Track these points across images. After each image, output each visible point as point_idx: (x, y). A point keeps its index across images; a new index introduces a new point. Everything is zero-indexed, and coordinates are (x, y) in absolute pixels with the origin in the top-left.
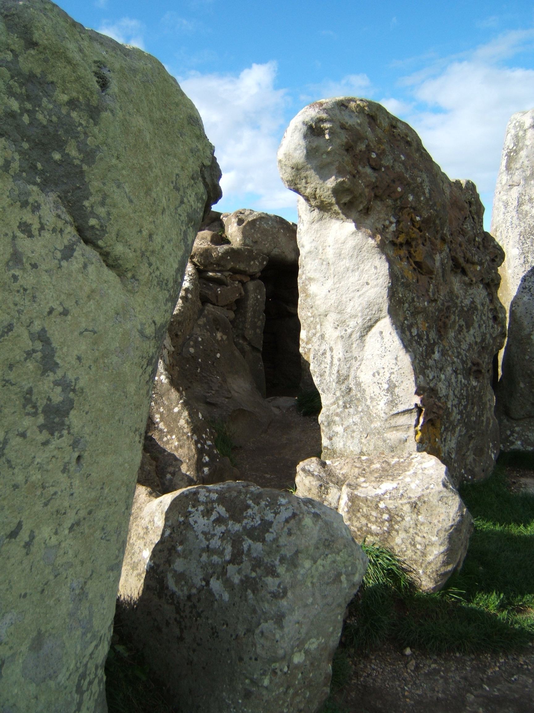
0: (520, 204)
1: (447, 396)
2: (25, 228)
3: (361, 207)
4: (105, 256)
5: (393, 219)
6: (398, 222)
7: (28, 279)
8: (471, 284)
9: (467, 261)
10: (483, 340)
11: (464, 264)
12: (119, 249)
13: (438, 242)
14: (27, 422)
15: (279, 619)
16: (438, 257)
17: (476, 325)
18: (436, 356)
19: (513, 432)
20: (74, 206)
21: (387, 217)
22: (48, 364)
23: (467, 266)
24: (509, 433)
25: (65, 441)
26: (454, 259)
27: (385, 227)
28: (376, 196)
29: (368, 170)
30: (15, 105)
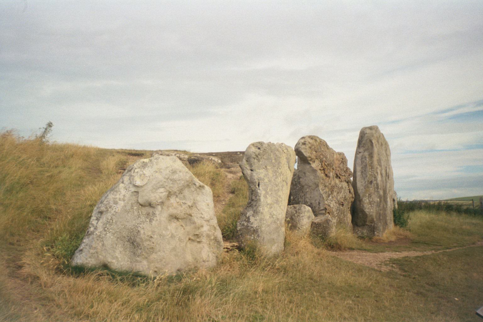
0: (362, 159)
6: (322, 164)
8: (342, 181)
9: (341, 175)
10: (345, 197)
11: (339, 176)
13: (332, 169)
16: (331, 173)
17: (343, 192)
18: (330, 197)
19: (358, 230)
23: (341, 177)
24: (357, 231)
26: (337, 174)
27: (318, 166)
28: (316, 158)
29: (315, 152)
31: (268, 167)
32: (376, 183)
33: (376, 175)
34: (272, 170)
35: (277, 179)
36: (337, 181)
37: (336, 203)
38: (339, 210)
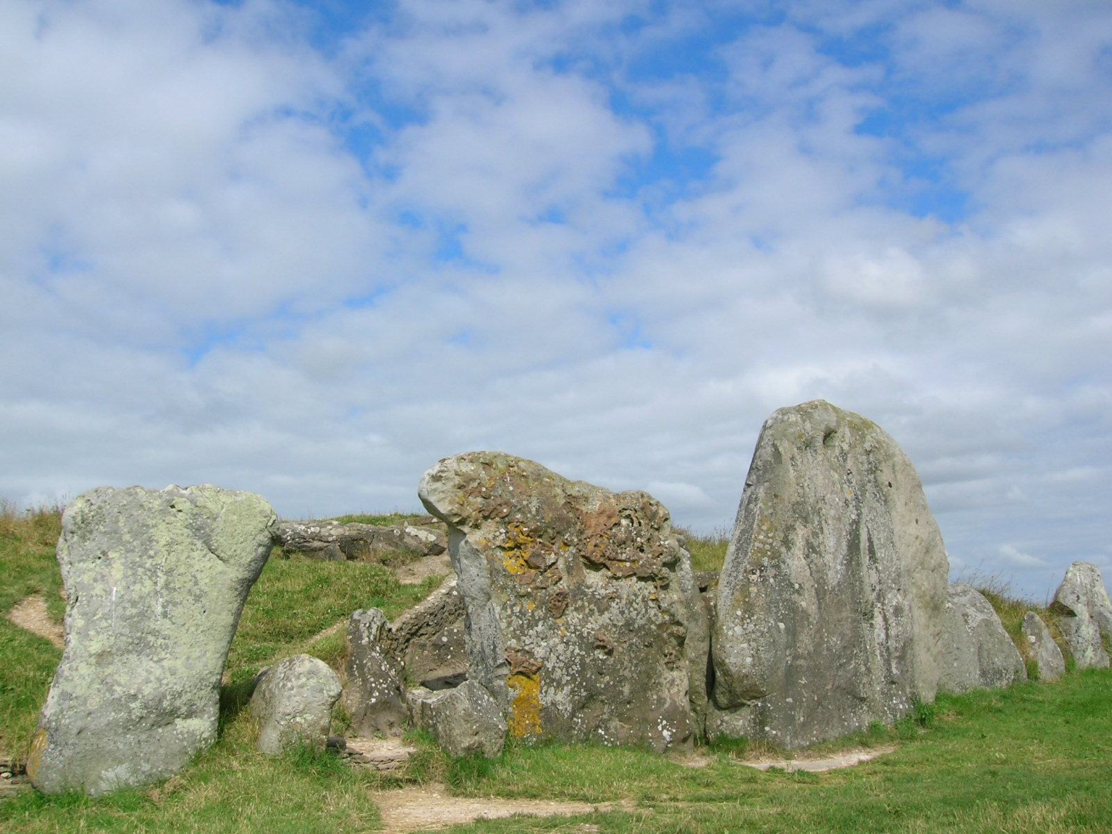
0: (749, 503)
1: (545, 659)
2: (192, 550)
3: (471, 524)
4: (218, 557)
5: (503, 531)
7: (192, 562)
12: (222, 555)
14: (189, 597)
15: (289, 697)
18: (540, 628)
20: (207, 543)
21: (497, 529)
22: (196, 583)
23: (608, 563)
24: (719, 722)
25: (200, 605)
29: (479, 500)
30: (191, 521)
31: (111, 554)
32: (775, 577)
33: (783, 549)
34: (123, 561)
35: (138, 587)
36: (594, 579)
37: (567, 643)
38: (583, 664)
